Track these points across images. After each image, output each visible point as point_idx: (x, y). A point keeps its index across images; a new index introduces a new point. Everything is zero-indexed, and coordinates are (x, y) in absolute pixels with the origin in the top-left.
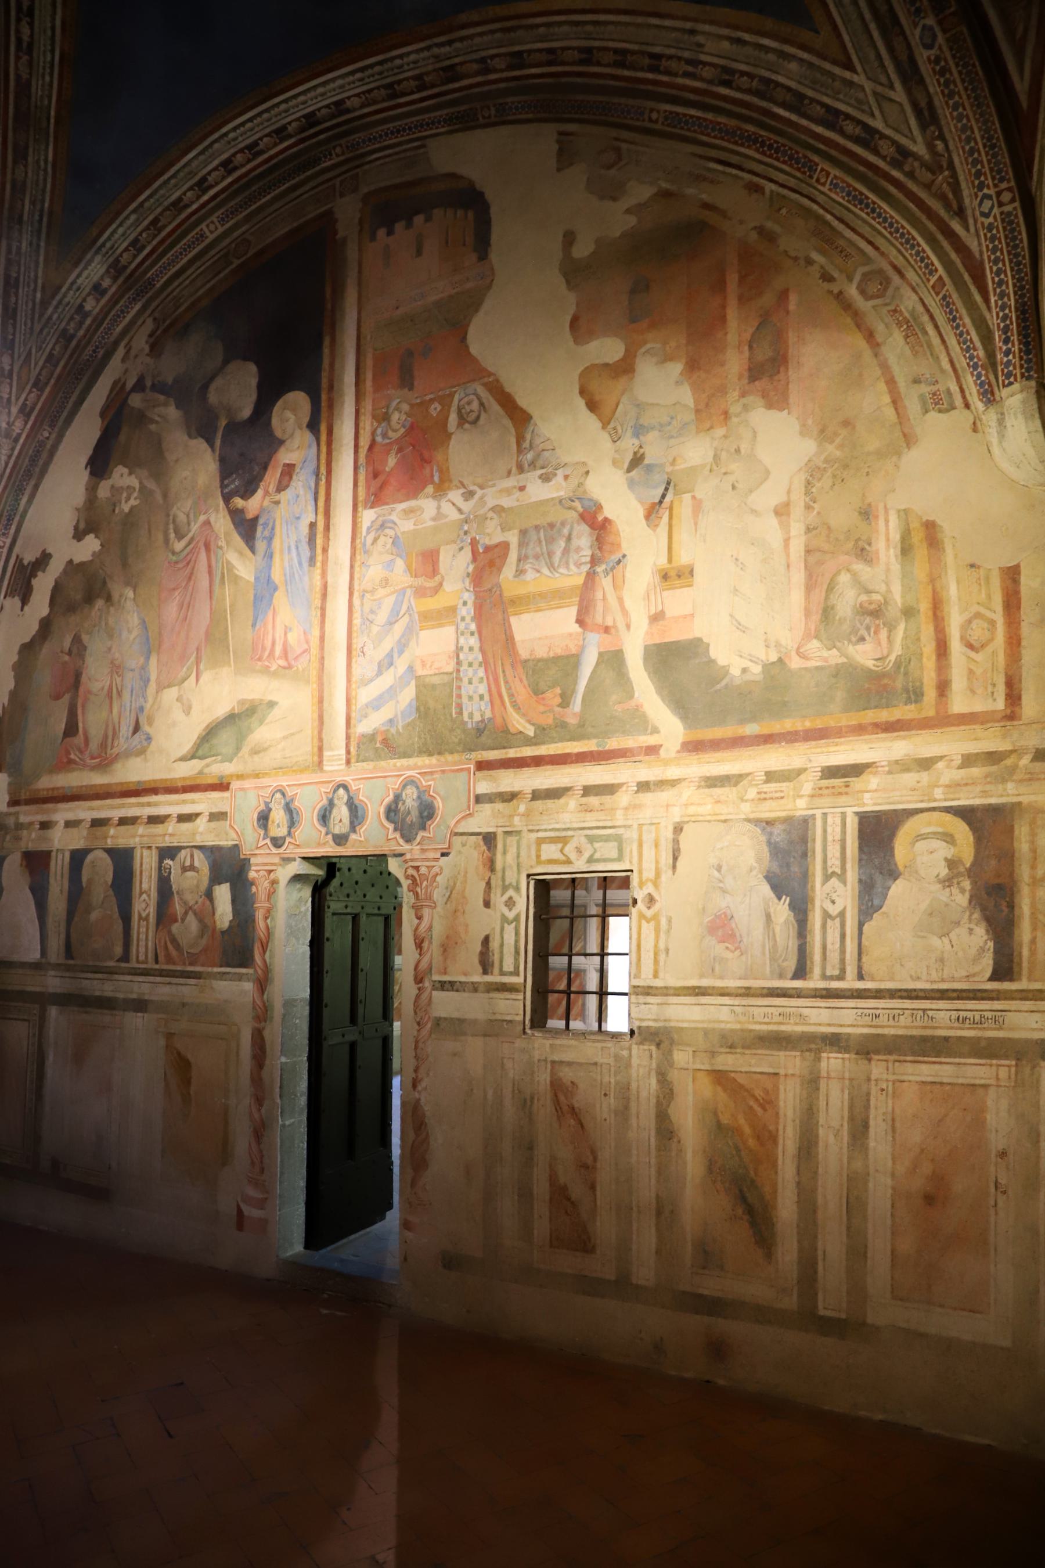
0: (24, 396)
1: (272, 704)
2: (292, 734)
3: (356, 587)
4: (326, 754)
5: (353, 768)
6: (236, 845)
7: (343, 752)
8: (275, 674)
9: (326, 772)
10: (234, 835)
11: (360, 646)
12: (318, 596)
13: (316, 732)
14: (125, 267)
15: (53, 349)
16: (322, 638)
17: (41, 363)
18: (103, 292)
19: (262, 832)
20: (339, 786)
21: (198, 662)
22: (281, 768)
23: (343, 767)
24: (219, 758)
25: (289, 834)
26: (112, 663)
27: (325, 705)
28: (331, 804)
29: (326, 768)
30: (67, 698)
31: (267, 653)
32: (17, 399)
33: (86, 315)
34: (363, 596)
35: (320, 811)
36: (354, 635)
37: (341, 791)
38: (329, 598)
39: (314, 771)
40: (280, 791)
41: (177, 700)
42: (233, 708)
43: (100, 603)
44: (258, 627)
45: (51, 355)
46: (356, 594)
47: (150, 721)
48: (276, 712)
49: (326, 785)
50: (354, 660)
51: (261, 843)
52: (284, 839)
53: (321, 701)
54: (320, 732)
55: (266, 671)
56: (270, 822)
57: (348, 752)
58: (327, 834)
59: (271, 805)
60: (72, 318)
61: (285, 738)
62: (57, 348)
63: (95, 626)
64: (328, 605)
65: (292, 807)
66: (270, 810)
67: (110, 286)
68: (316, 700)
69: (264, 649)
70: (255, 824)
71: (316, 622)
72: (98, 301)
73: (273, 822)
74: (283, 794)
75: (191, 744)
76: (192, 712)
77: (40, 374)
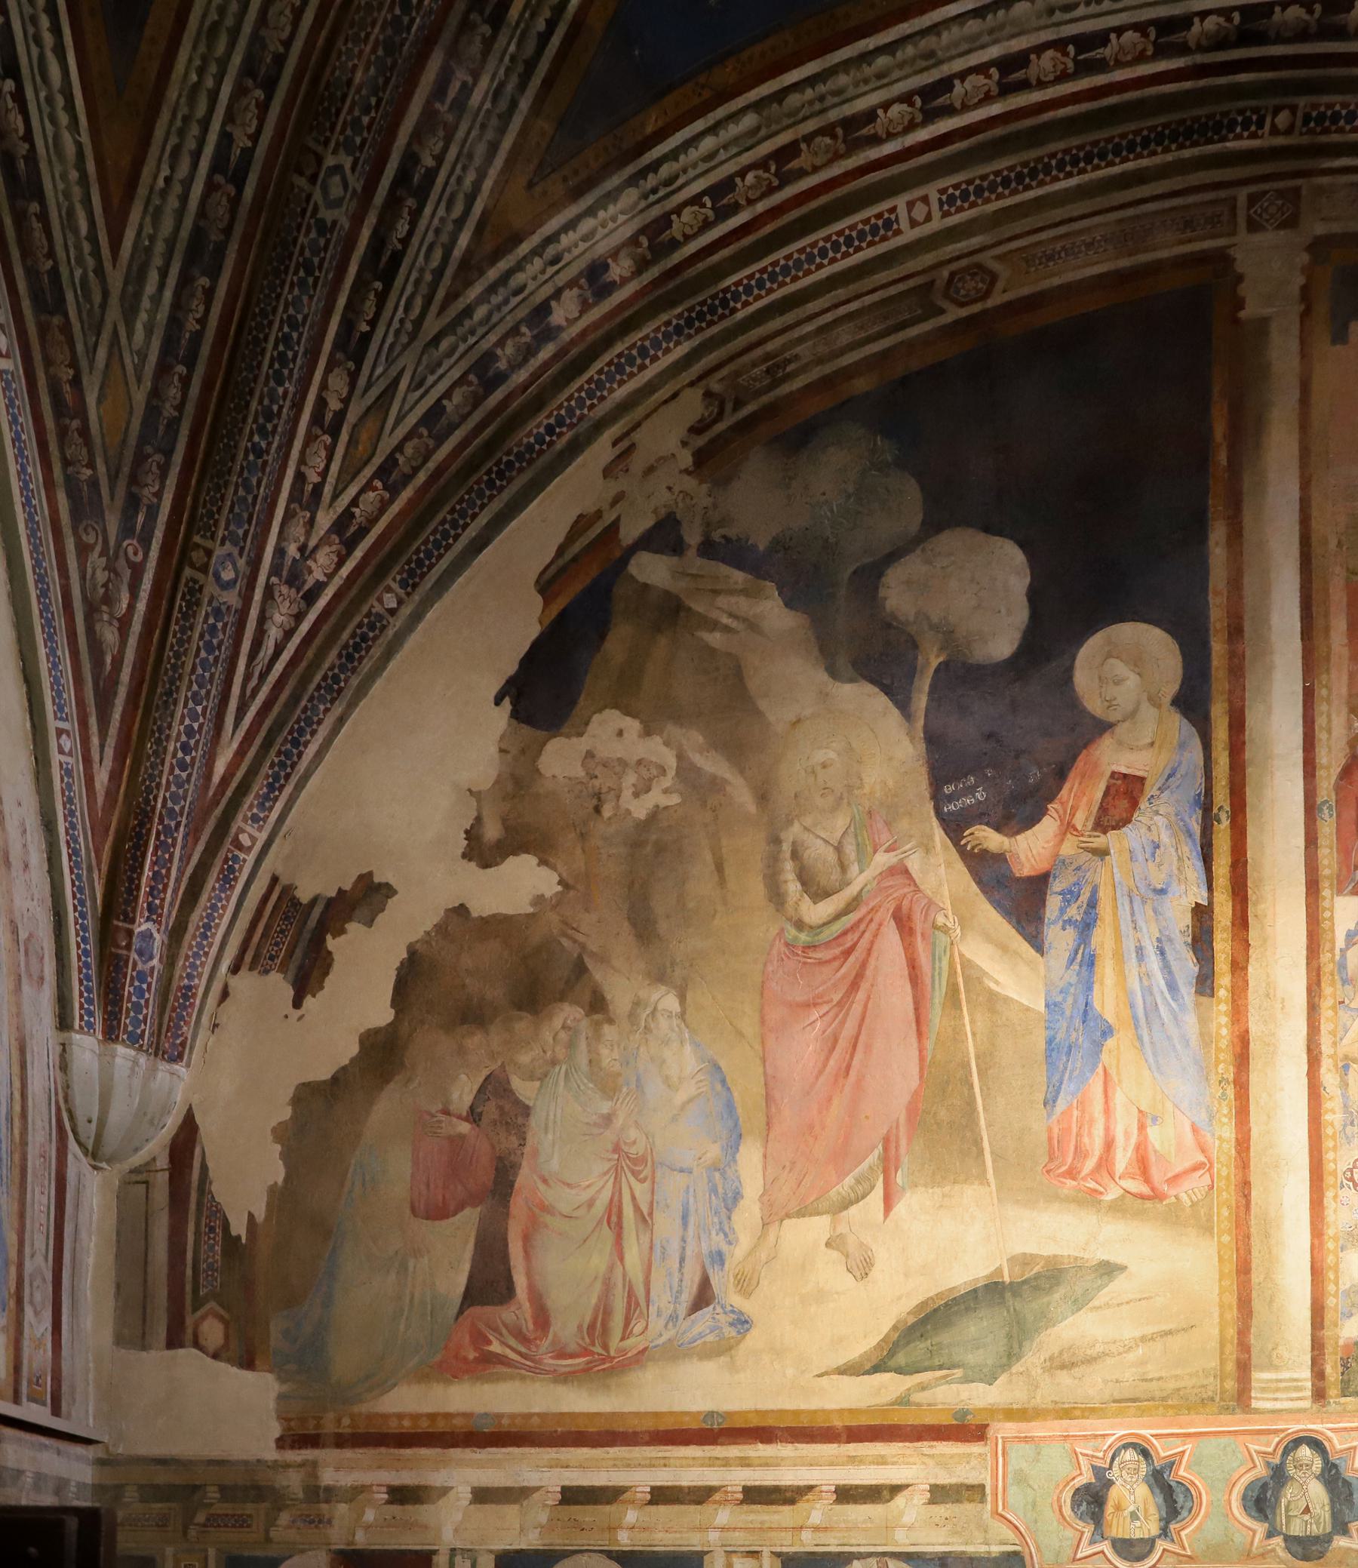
0: (352, 491)
1: (1108, 1270)
2: (1170, 1333)
3: (1326, 1048)
4: (1259, 1376)
5: (1332, 1408)
6: (1016, 1554)
7: (1307, 1373)
8: (1117, 1208)
9: (1257, 1411)
10: (1010, 1535)
11: (1342, 1167)
12: (1226, 1056)
13: (1232, 1332)
14: (674, 245)
15: (448, 394)
16: (1243, 1144)
17: (412, 420)
18: (604, 290)
19: (1088, 1530)
20: (1297, 1442)
21: (888, 1165)
22: (1134, 1400)
23: (1307, 1404)
24: (958, 1373)
25: (1165, 1532)
26: (617, 1149)
27: (1256, 1277)
28: (1279, 1476)
29: (1254, 1404)
30: (468, 1220)
31: (1090, 1164)
32: (335, 496)
33: (548, 334)
34: (1346, 1067)
35: (1249, 1487)
36: (1328, 1144)
37: (1305, 1452)
38: (1255, 1065)
39: (1226, 1410)
40: (1134, 1446)
41: (828, 1245)
42: (999, 1271)
43: (569, 1013)
44: (1061, 1105)
45: (437, 410)
46: (1326, 1064)
47: (746, 1284)
48: (1119, 1286)
49: (1264, 1438)
50: (1329, 1194)
51: (1085, 1550)
52: (1151, 1543)
53: (1244, 1269)
54: (1243, 1332)
55: (1090, 1199)
56: (1109, 1509)
57: (1318, 1374)
58: (1270, 1535)
59: (1114, 1474)
60: (514, 331)
61: (1143, 1339)
62: (457, 397)
63: (554, 1062)
64: (1254, 1077)
65: (1171, 1478)
66: (1110, 1483)
67: (624, 281)
68: (1231, 1267)
69: (1080, 1153)
70: (1067, 1511)
71: (1226, 1111)
72: (585, 307)
73: (1118, 1508)
74: (1145, 1453)
75: (874, 1340)
76: (875, 1273)
77: (399, 448)
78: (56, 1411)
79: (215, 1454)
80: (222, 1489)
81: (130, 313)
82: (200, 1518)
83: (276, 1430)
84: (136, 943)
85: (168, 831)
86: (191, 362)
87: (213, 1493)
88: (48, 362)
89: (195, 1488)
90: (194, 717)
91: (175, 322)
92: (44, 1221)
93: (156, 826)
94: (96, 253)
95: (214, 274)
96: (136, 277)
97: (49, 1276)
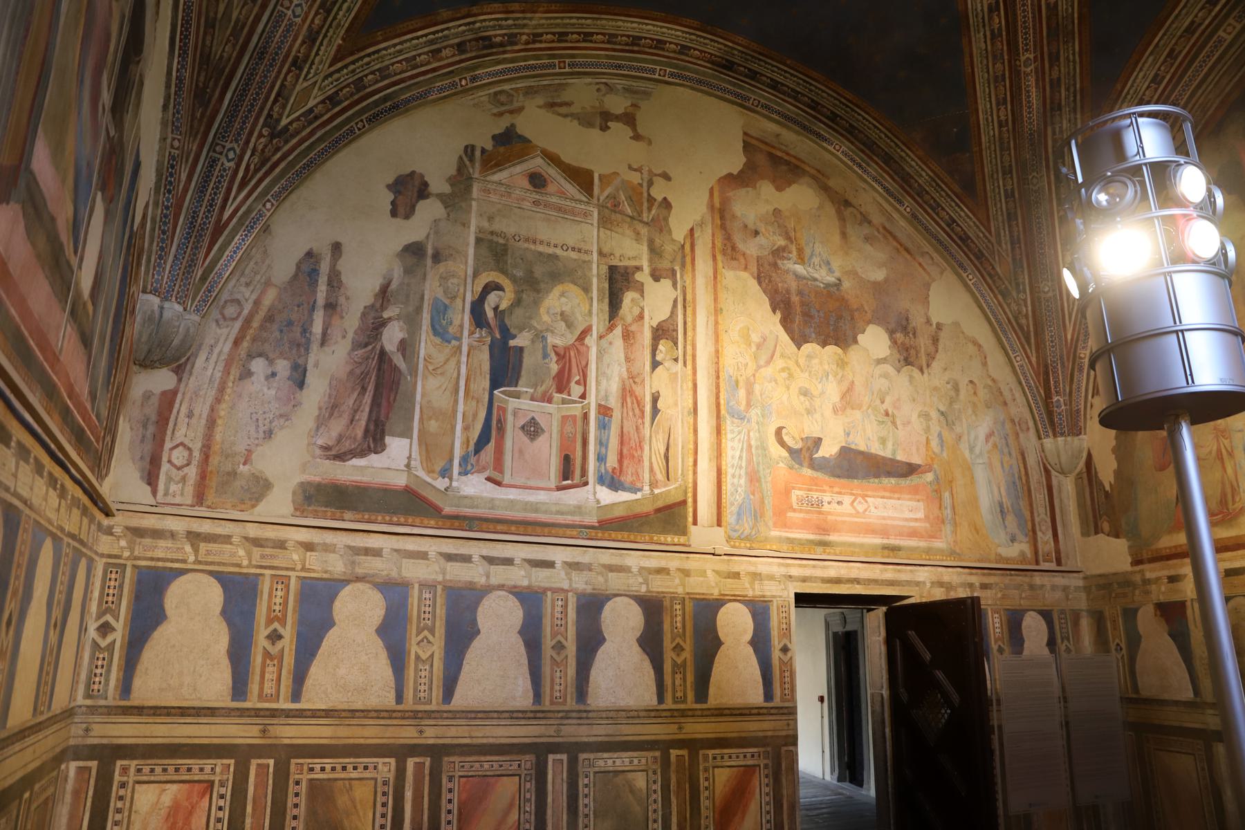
78: (1059, 563)
79: (1113, 570)
80: (1118, 584)
81: (999, 243)
82: (1113, 595)
83: (1129, 560)
84: (1055, 404)
85: (1054, 367)
86: (1019, 242)
87: (1115, 586)
88: (985, 269)
89: (1110, 584)
90: (1051, 331)
91: (1011, 236)
92: (1043, 502)
93: (1050, 368)
94: (987, 238)
95: (1017, 219)
96: (998, 235)
97: (1049, 520)
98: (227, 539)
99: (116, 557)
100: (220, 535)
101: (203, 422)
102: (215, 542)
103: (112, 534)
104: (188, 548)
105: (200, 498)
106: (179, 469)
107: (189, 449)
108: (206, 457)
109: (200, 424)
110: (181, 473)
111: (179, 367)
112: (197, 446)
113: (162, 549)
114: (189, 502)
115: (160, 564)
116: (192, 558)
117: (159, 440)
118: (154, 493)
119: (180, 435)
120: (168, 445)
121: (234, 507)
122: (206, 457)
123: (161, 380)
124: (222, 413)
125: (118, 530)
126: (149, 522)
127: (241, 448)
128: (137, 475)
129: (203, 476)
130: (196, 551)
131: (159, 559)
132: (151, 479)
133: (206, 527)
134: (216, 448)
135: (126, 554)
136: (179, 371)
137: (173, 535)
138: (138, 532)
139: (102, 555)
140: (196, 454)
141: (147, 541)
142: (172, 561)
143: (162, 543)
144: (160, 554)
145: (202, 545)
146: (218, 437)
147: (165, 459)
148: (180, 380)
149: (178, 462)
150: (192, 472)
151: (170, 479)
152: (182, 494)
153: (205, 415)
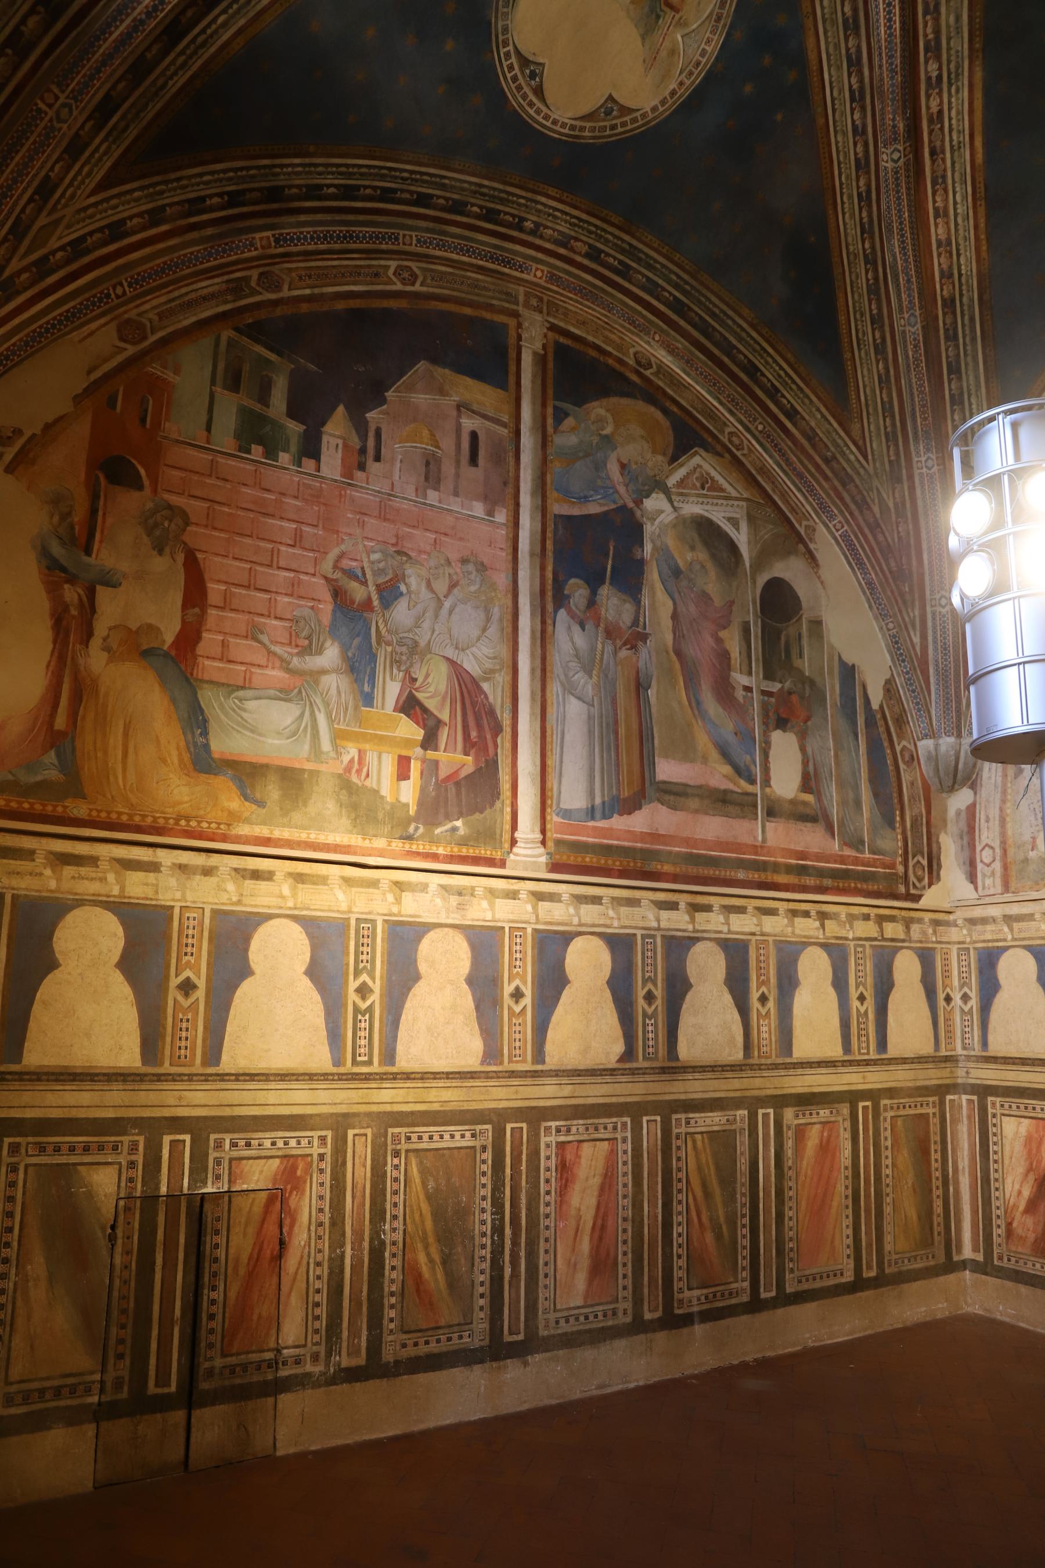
98: (1030, 917)
99: (963, 943)
100: (1026, 915)
101: (997, 822)
102: (1023, 921)
103: (957, 926)
104: (1006, 929)
105: (1006, 887)
106: (988, 865)
107: (992, 848)
108: (1005, 852)
109: (995, 824)
110: (991, 869)
111: (972, 783)
112: (996, 844)
113: (989, 933)
114: (1000, 891)
115: (990, 945)
116: (1010, 937)
117: (972, 846)
118: (976, 889)
119: (985, 839)
120: (978, 848)
121: (1031, 889)
122: (1005, 852)
123: (961, 799)
124: (1009, 811)
125: (960, 922)
126: (977, 913)
127: (1027, 837)
128: (963, 877)
129: (1005, 867)
130: (1011, 930)
131: (989, 941)
132: (972, 878)
133: (1015, 910)
134: (1010, 841)
135: (968, 940)
136: (973, 787)
137: (994, 920)
138: (972, 922)
139: (955, 943)
140: (998, 851)
141: (979, 927)
142: (997, 941)
143: (989, 927)
144: (989, 937)
145: (1015, 924)
146: (1010, 833)
147: (978, 860)
148: (975, 794)
149: (987, 861)
150: (997, 866)
151: (984, 875)
152: (994, 886)
153: (997, 818)
